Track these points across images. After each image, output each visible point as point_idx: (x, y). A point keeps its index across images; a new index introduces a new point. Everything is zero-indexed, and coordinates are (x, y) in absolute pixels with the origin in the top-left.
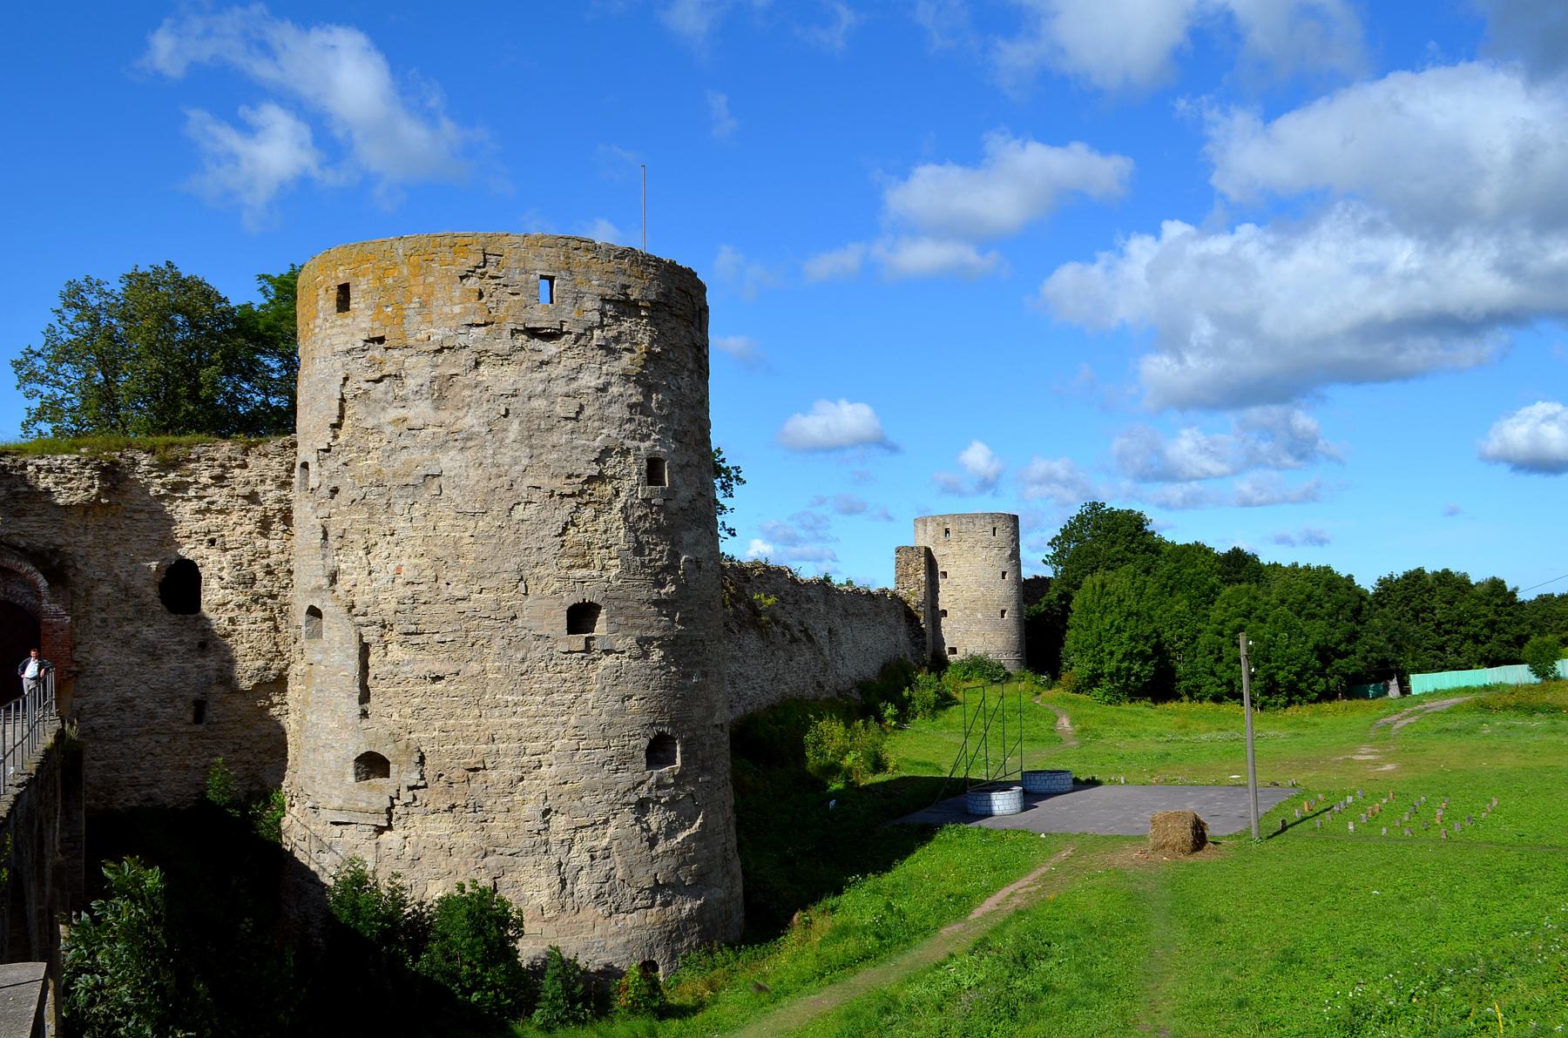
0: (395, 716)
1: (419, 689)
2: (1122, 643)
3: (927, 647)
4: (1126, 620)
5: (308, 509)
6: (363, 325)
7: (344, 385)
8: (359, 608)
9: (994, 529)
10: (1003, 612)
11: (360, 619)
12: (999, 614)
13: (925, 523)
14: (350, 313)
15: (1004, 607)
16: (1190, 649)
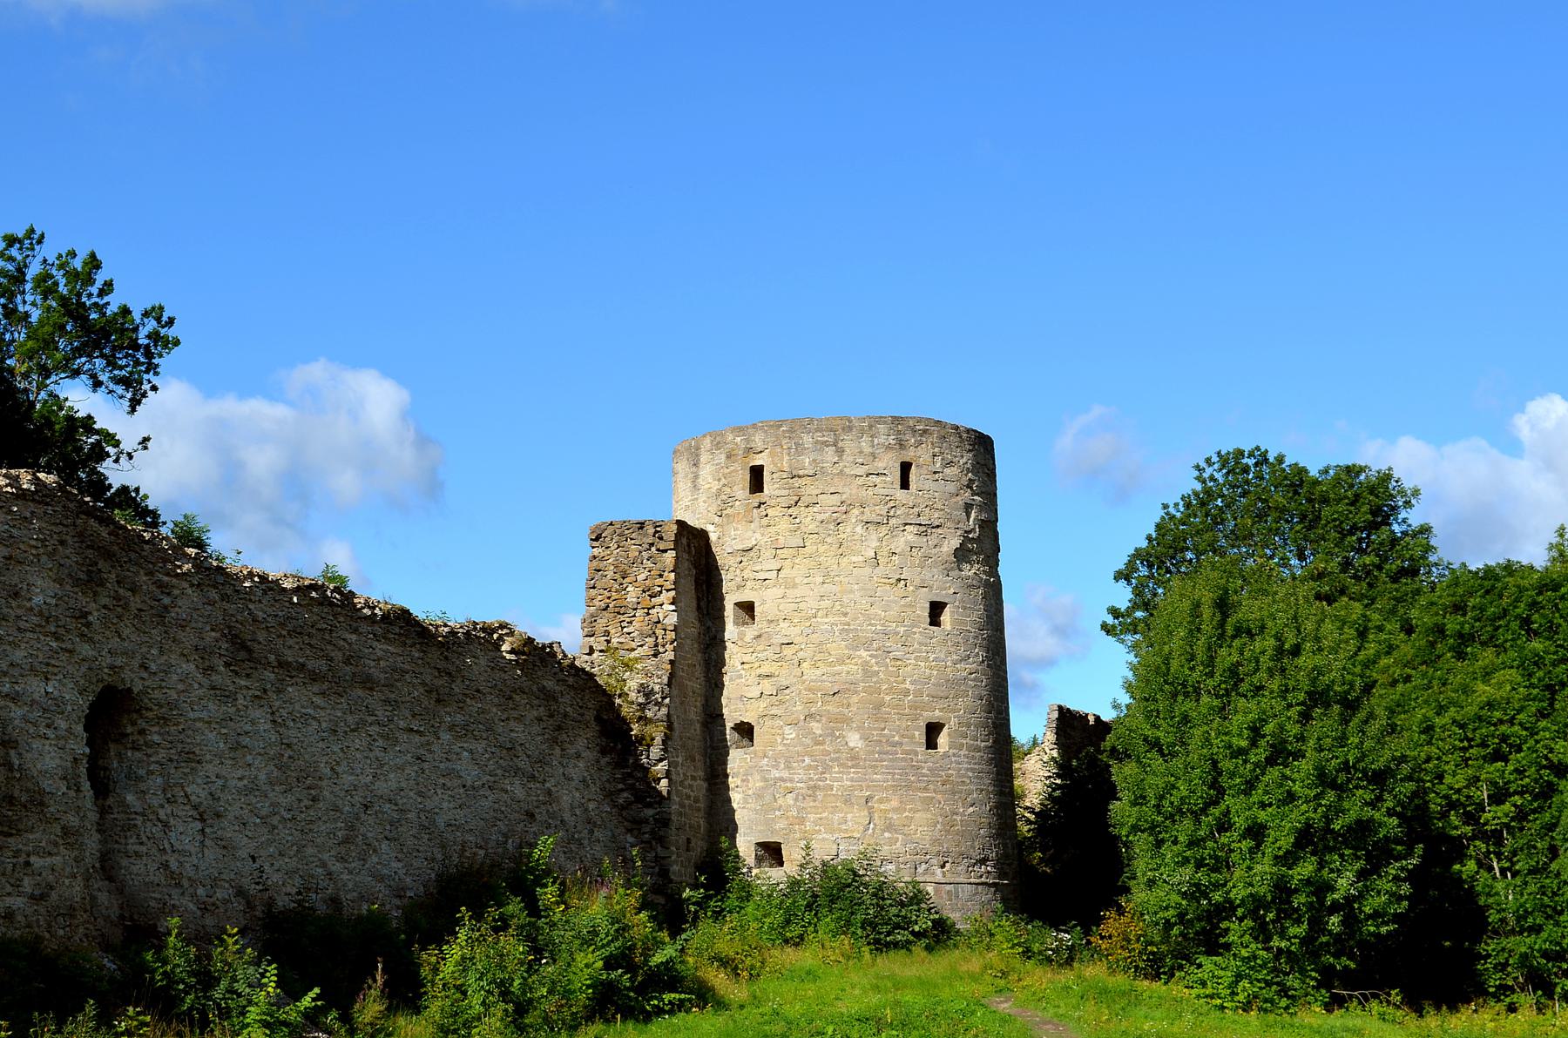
2: (1291, 797)
4: (1306, 717)
9: (905, 468)
10: (933, 730)
12: (920, 736)
15: (936, 715)
16: (1533, 826)
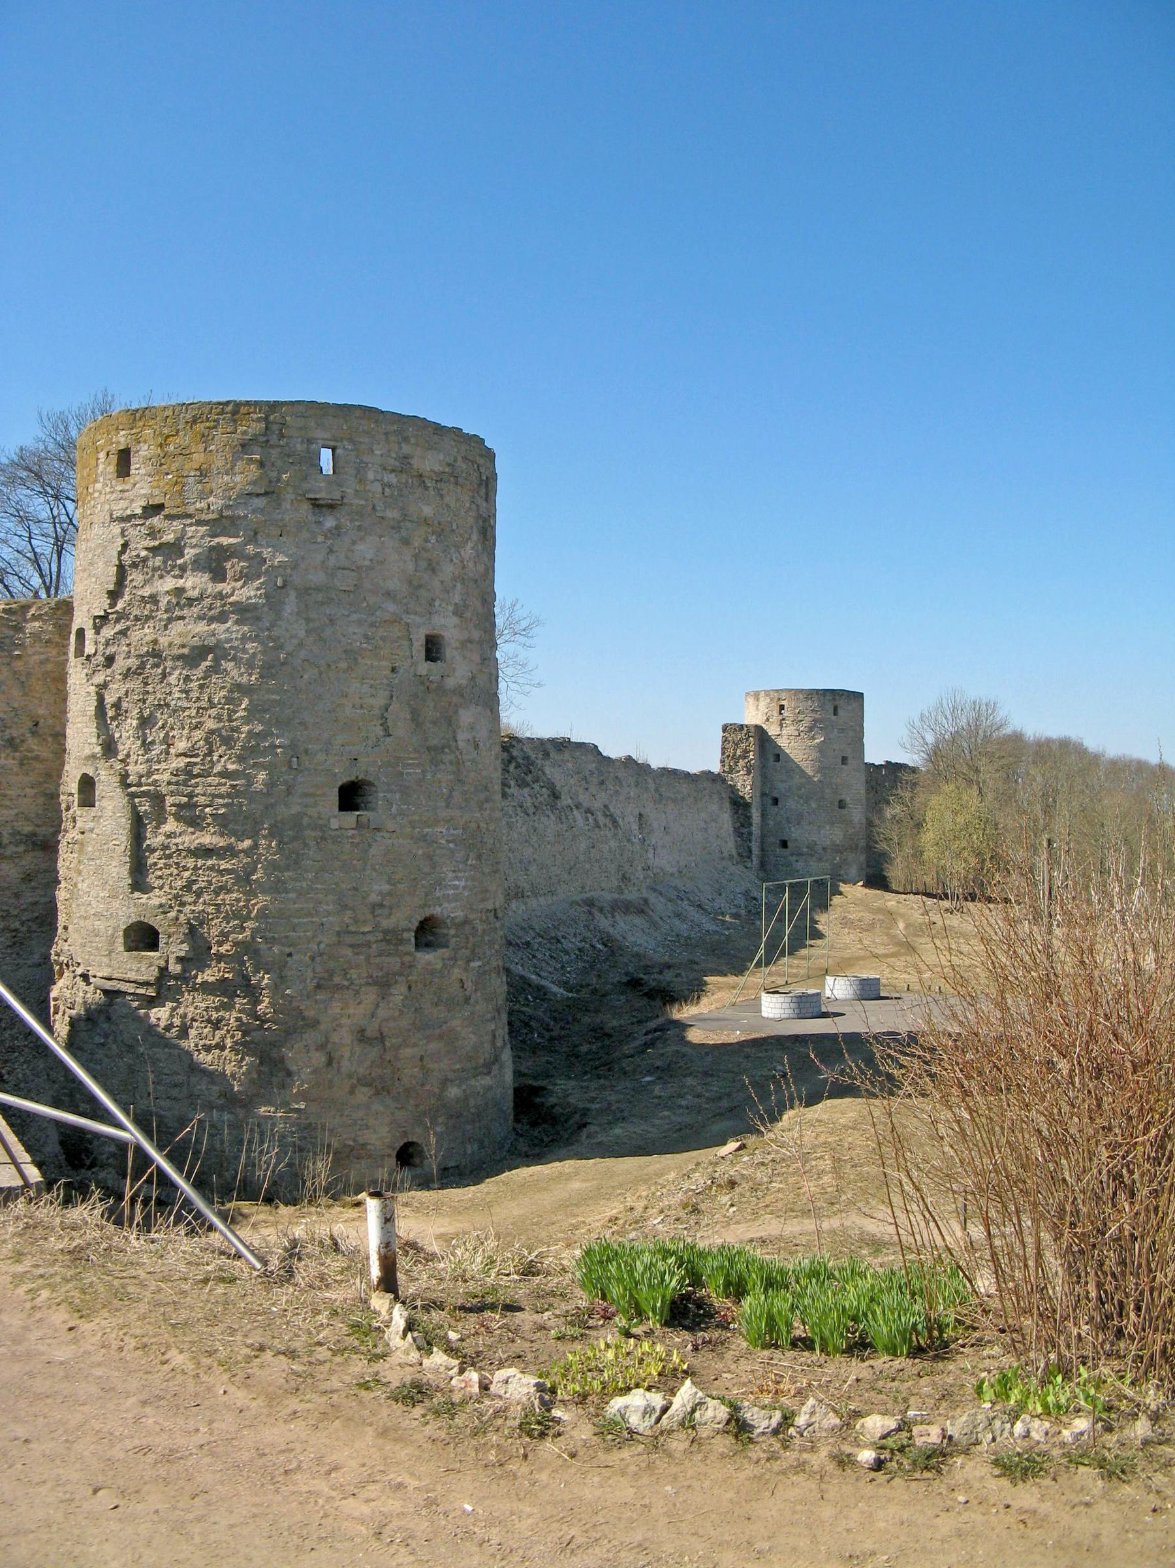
0: (166, 888)
1: (190, 862)
3: (753, 838)
5: (83, 676)
6: (143, 492)
7: (121, 553)
8: (132, 779)
11: (133, 789)
13: (756, 696)
14: (131, 480)
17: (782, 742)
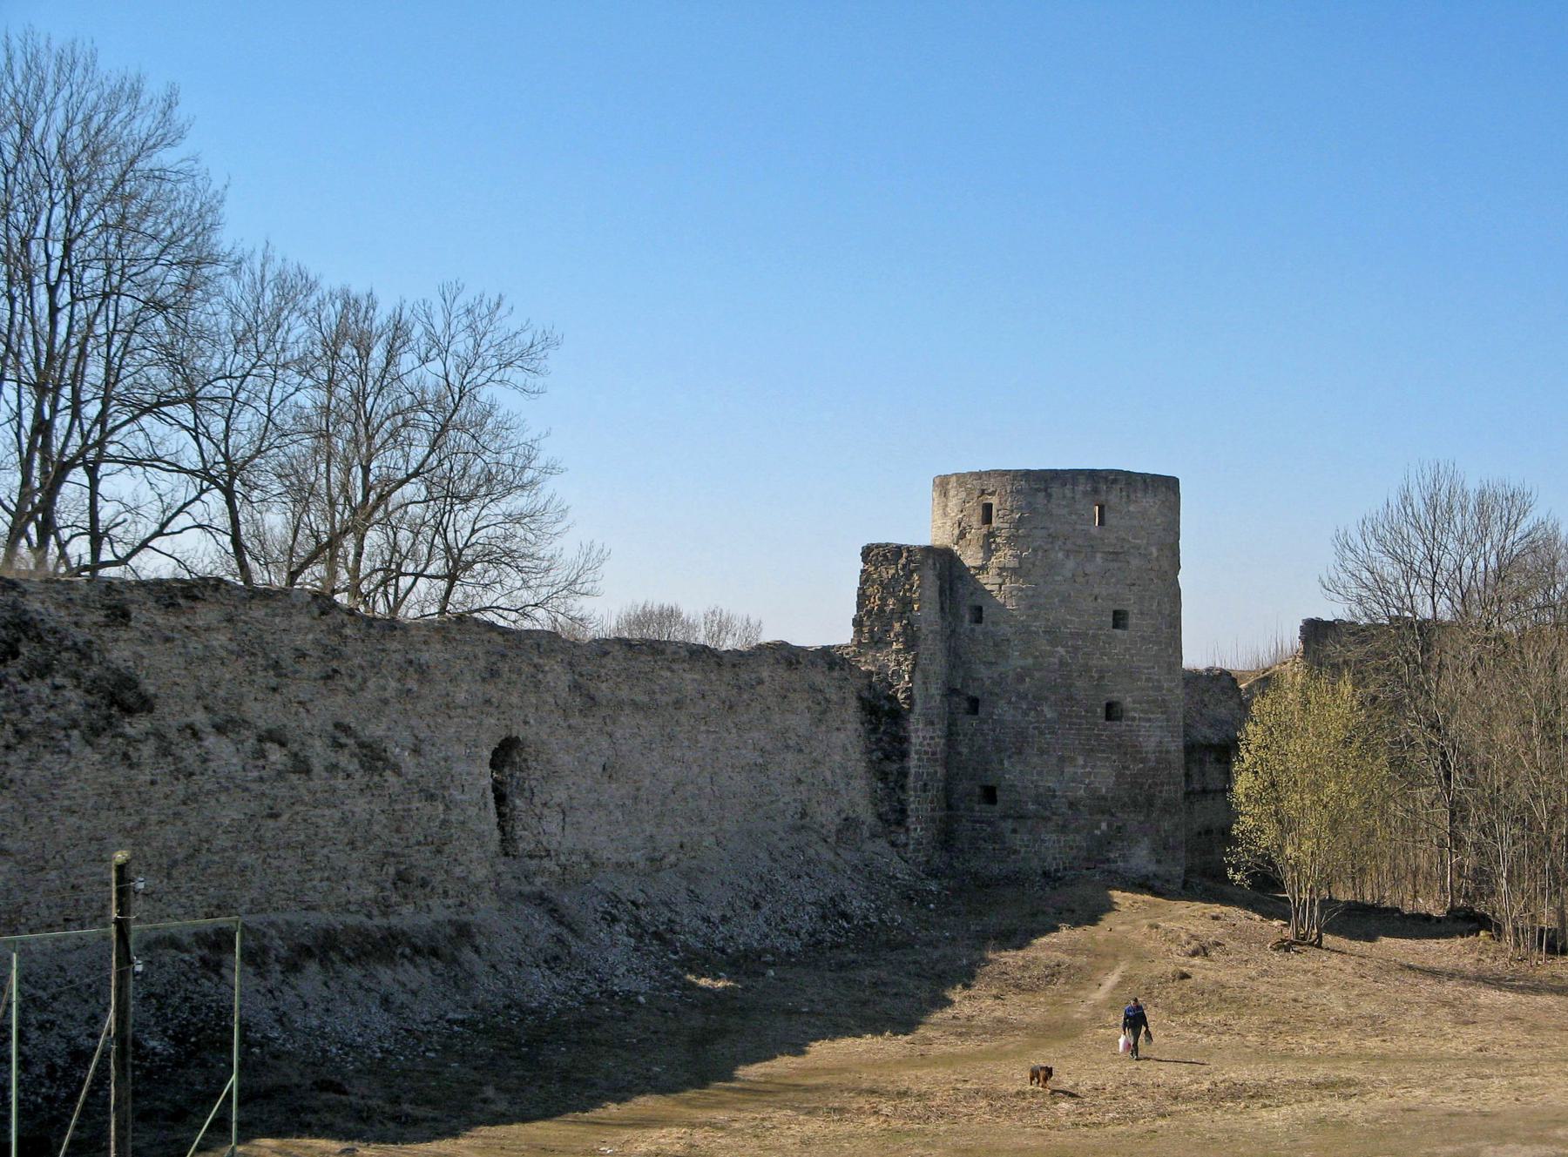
17: (989, 581)
